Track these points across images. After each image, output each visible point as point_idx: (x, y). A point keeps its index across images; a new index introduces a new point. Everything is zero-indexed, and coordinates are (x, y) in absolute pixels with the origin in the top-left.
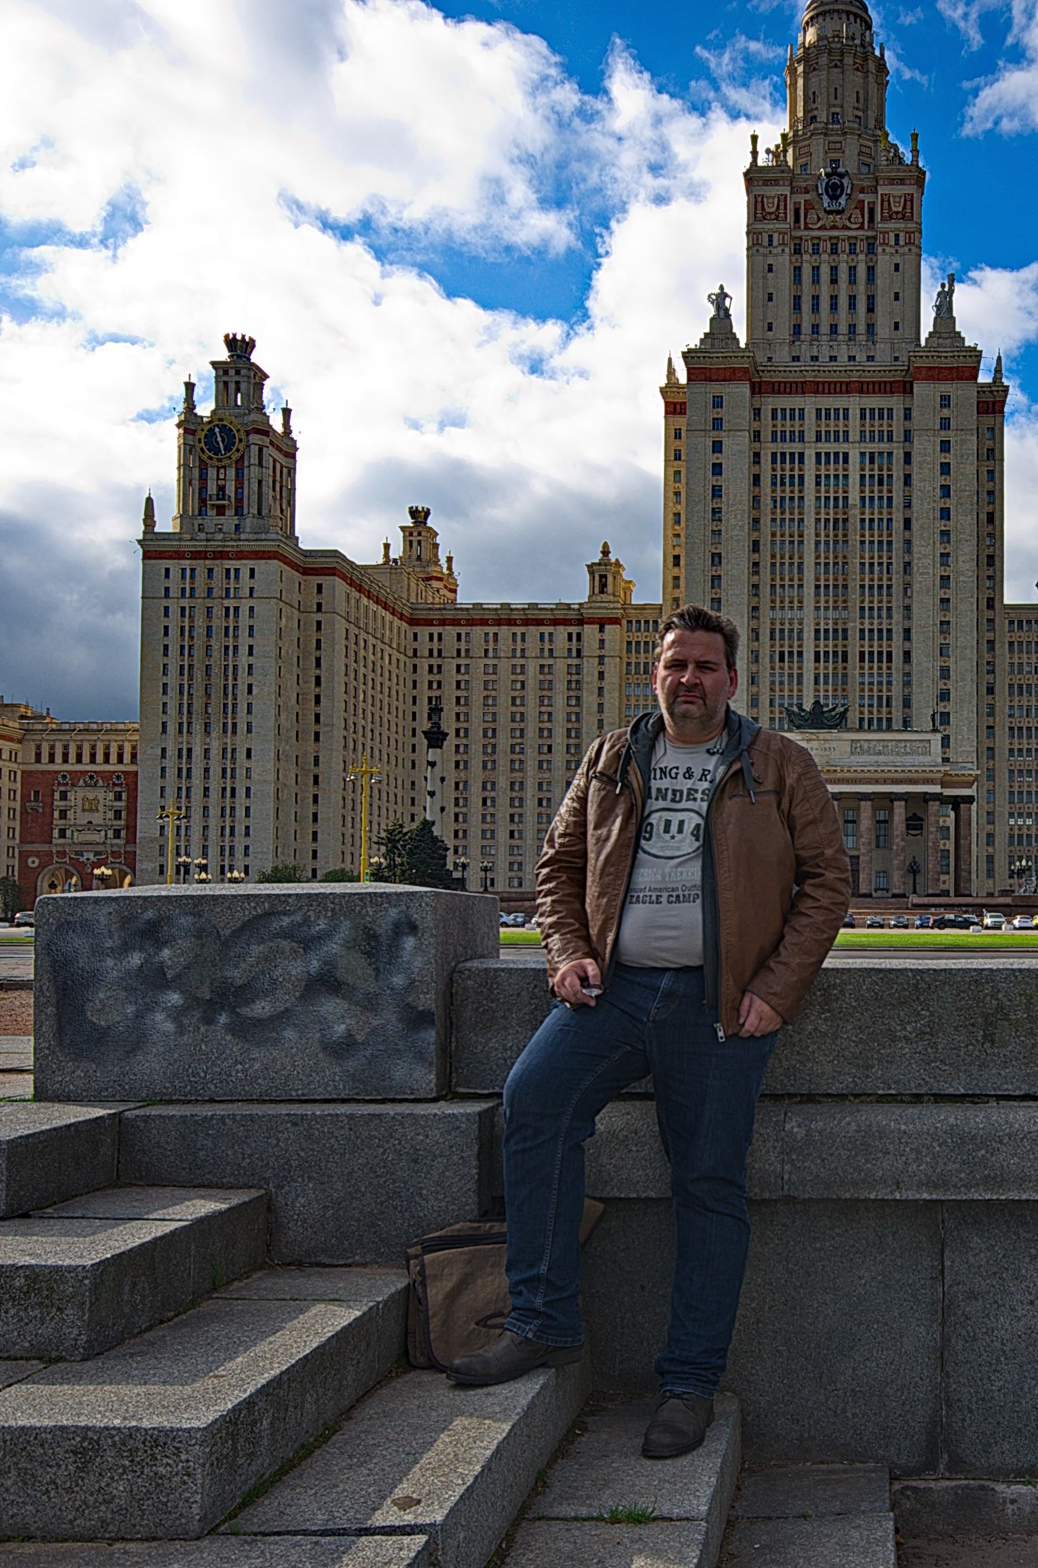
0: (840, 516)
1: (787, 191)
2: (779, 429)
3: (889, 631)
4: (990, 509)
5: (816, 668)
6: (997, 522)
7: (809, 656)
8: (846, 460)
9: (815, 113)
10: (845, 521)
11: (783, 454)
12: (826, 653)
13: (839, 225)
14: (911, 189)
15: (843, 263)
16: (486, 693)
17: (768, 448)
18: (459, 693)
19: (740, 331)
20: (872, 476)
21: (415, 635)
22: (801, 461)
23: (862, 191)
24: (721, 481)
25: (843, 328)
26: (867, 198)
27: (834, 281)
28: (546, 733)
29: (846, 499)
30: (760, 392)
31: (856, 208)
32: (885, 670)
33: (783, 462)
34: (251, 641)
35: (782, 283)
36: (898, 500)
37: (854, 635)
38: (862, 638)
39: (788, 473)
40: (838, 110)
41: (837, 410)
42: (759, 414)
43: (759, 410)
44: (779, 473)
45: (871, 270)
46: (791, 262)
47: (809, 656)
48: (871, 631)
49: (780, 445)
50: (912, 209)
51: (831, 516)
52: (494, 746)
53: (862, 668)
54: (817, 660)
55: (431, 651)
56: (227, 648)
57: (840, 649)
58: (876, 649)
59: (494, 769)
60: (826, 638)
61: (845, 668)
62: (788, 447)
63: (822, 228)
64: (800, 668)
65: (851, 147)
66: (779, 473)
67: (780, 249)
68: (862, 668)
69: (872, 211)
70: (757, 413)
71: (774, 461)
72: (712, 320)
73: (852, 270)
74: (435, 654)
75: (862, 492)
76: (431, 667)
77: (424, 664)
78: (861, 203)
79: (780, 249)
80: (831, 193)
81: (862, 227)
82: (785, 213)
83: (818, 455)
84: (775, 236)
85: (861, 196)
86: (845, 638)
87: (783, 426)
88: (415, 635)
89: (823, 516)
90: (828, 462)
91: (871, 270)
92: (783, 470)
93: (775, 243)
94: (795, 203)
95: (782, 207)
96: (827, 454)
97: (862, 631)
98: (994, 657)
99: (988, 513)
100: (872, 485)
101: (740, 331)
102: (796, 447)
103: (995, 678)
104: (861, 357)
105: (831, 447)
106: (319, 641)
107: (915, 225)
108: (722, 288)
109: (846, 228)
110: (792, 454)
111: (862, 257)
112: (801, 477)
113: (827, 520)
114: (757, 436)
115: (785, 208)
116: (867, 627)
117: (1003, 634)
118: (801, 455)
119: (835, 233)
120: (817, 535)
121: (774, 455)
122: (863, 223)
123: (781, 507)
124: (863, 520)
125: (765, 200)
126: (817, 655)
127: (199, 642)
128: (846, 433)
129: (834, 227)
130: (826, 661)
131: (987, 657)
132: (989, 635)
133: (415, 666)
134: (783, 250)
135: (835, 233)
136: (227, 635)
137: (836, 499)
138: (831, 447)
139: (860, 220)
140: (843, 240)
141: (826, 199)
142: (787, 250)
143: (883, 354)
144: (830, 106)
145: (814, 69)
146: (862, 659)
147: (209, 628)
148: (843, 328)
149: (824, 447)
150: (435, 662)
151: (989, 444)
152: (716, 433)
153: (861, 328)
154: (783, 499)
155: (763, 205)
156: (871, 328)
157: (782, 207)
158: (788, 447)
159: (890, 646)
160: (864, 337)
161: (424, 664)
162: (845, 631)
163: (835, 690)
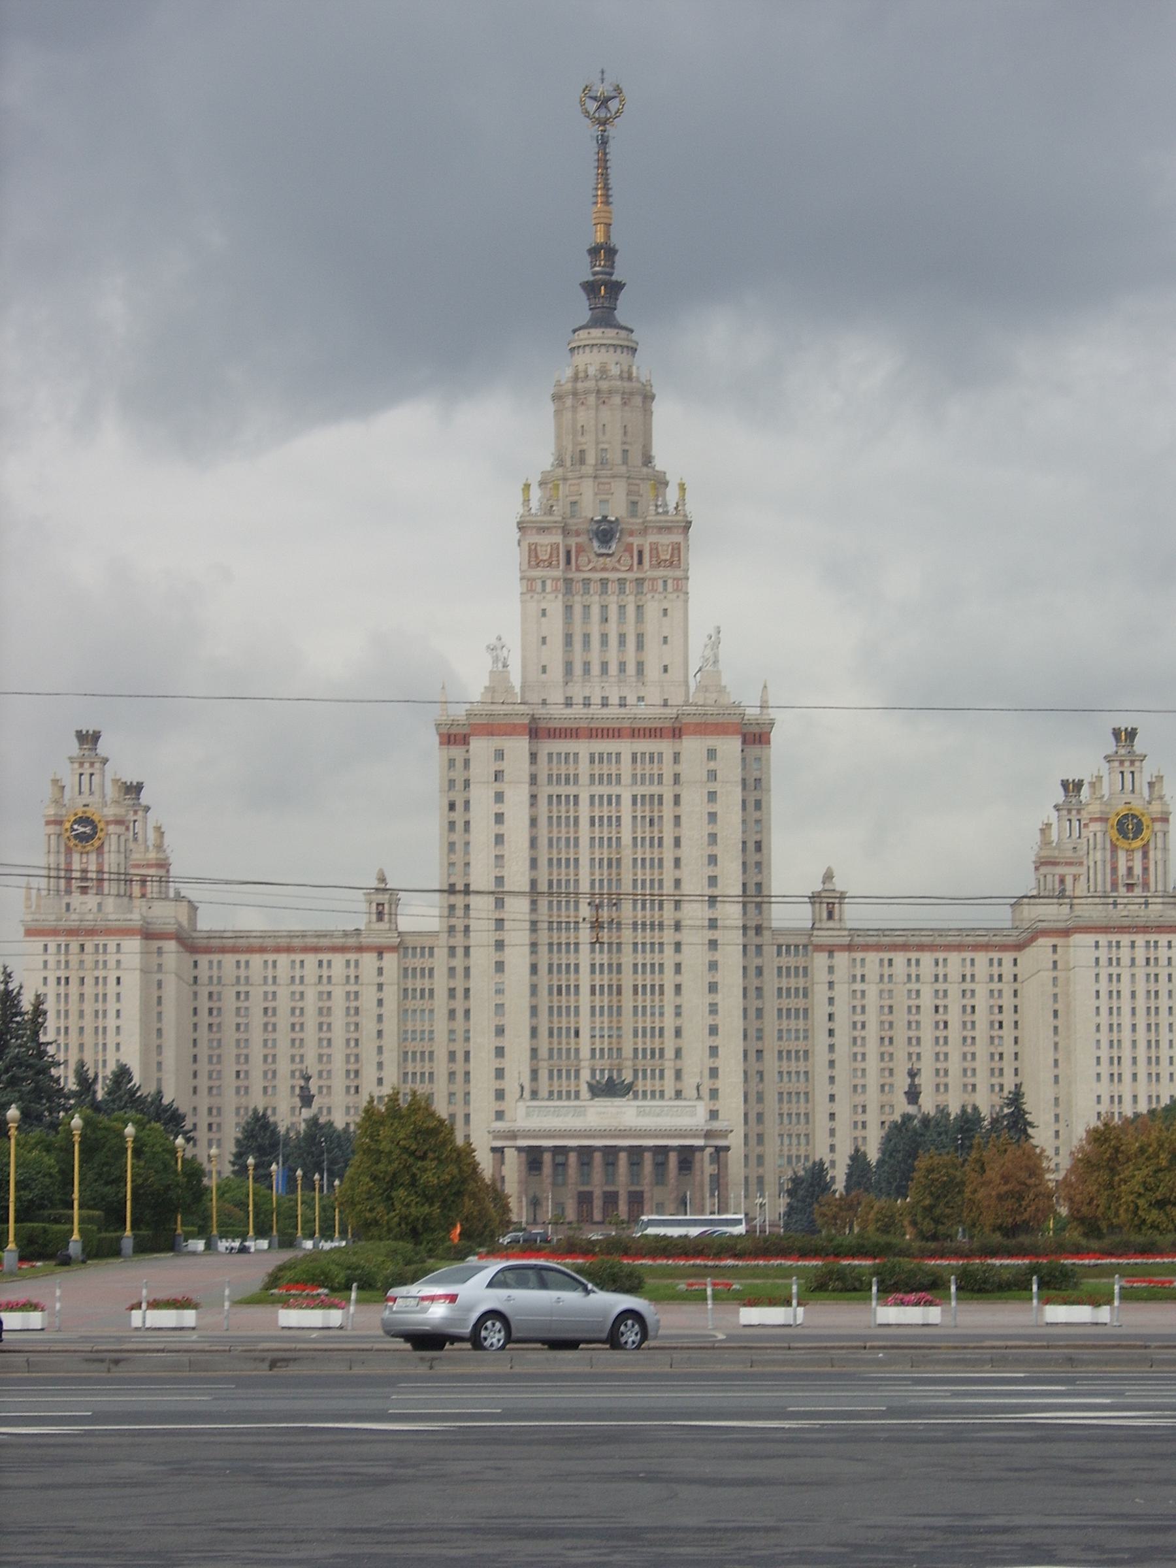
0: (614, 856)
1: (558, 538)
2: (555, 772)
3: (661, 965)
4: (757, 837)
5: (592, 1001)
6: (764, 851)
7: (585, 990)
8: (618, 803)
9: (584, 447)
10: (619, 860)
11: (559, 796)
12: (602, 986)
13: (609, 566)
14: (677, 538)
15: (613, 601)
16: (266, 1020)
17: (544, 791)
18: (240, 1020)
19: (516, 679)
20: (643, 817)
21: (196, 962)
22: (576, 803)
23: (631, 534)
24: (503, 829)
25: (613, 669)
26: (636, 541)
27: (605, 620)
28: (325, 1059)
29: (619, 839)
30: (536, 736)
31: (625, 551)
32: (657, 1003)
33: (559, 802)
34: (118, 1006)
35: (554, 626)
36: (668, 841)
37: (627, 970)
38: (635, 972)
39: (563, 815)
40: (605, 446)
41: (610, 754)
42: (536, 758)
43: (536, 754)
44: (555, 815)
45: (639, 608)
46: (564, 603)
47: (585, 990)
48: (644, 965)
49: (557, 788)
50: (679, 556)
51: (605, 856)
52: (274, 1072)
53: (636, 1001)
54: (593, 992)
55: (211, 978)
56: (97, 1012)
57: (614, 982)
58: (648, 983)
59: (274, 1094)
60: (602, 972)
61: (619, 1001)
62: (563, 790)
63: (593, 570)
64: (577, 1001)
65: (619, 490)
66: (555, 815)
67: (551, 597)
68: (636, 1001)
69: (640, 553)
70: (533, 757)
71: (550, 802)
72: (491, 672)
73: (622, 608)
74: (215, 980)
75: (635, 832)
76: (211, 994)
77: (204, 992)
78: (629, 548)
79: (554, 595)
80: (600, 535)
81: (630, 569)
82: (558, 560)
83: (592, 797)
84: (549, 583)
85: (630, 540)
86: (619, 971)
87: (559, 769)
88: (196, 962)
89: (597, 856)
90: (601, 804)
91: (639, 608)
92: (559, 811)
93: (548, 589)
94: (566, 546)
95: (555, 553)
96: (601, 797)
97: (635, 965)
98: (762, 982)
99: (756, 842)
100: (643, 826)
101: (516, 679)
102: (571, 790)
103: (763, 1003)
104: (631, 699)
105: (604, 790)
106: (160, 998)
107: (682, 573)
108: (499, 639)
109: (614, 569)
110: (567, 797)
111: (631, 598)
112: (576, 819)
113: (601, 860)
114: (533, 779)
115: (558, 556)
116: (640, 961)
117: (771, 960)
118: (576, 797)
119: (605, 575)
120: (592, 874)
121: (550, 797)
122: (632, 565)
123: (557, 847)
124: (635, 860)
125: (539, 548)
126: (593, 988)
127: (73, 1007)
128: (619, 776)
129: (604, 569)
130: (602, 993)
131: (756, 982)
132: (758, 961)
133: (195, 994)
134: (556, 597)
135: (605, 575)
136: (97, 1000)
137: (610, 839)
138: (604, 790)
139: (630, 562)
140: (613, 581)
141: (596, 544)
142: (560, 596)
143: (654, 696)
144: (597, 443)
145: (583, 403)
146: (635, 992)
147: (82, 995)
148: (613, 669)
149: (598, 790)
150: (215, 989)
151: (756, 774)
152: (497, 785)
153: (631, 669)
154: (559, 839)
155: (536, 553)
156: (640, 666)
157: (555, 553)
158: (563, 790)
159: (662, 980)
160: (634, 679)
161: (204, 992)
162: (619, 965)
163: (611, 1022)
